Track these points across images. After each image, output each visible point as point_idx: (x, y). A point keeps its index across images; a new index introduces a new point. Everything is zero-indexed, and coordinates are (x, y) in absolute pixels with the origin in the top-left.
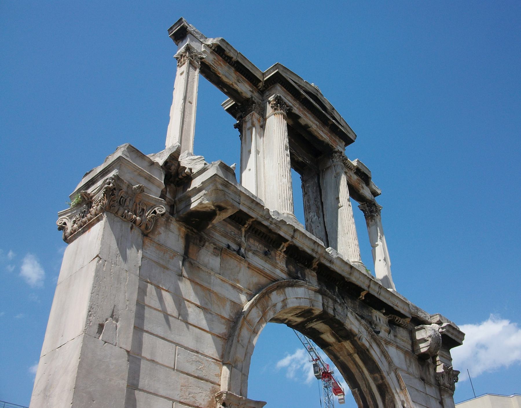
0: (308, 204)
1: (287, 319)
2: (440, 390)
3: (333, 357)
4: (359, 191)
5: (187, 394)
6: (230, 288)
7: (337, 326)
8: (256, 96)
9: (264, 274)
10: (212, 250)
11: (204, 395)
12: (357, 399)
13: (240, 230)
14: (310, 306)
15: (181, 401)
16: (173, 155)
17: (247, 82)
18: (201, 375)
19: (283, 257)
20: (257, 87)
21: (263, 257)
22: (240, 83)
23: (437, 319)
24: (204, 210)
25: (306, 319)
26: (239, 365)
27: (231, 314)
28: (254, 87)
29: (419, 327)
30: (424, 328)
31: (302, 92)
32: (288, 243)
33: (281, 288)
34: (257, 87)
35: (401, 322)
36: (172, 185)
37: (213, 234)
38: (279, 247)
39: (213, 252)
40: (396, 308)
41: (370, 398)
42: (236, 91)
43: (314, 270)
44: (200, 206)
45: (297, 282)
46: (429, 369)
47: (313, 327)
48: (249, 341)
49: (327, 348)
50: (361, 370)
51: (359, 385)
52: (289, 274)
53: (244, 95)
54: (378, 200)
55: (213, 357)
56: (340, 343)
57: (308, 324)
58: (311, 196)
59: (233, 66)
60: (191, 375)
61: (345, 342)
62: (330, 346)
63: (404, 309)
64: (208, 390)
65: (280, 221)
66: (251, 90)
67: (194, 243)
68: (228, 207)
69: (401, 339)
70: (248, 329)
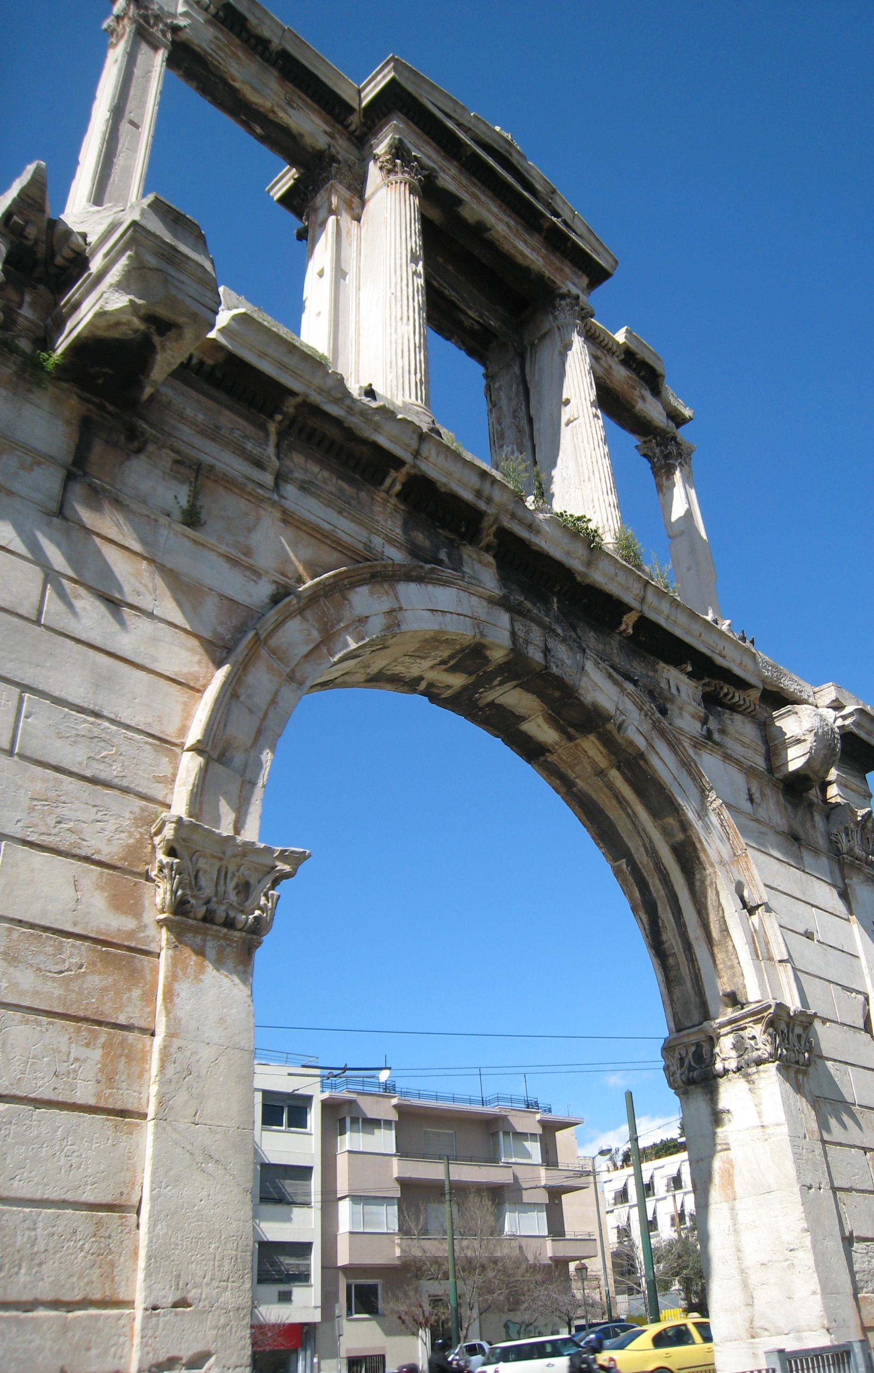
0: (499, 429)
1: (421, 678)
3: (558, 782)
4: (634, 407)
5: (51, 820)
6: (221, 563)
7: (557, 694)
8: (342, 148)
9: (333, 541)
10: (169, 465)
11: (111, 826)
12: (627, 886)
13: (263, 428)
14: (473, 634)
15: (28, 839)
16: (28, 196)
17: (315, 110)
19: (395, 510)
20: (346, 127)
21: (329, 501)
23: (830, 696)
24: (116, 334)
25: (473, 678)
26: (239, 758)
27: (220, 629)
28: (336, 125)
29: (783, 710)
30: (796, 713)
31: (462, 135)
32: (404, 470)
33: (385, 581)
34: (346, 127)
35: (736, 699)
36: (41, 287)
38: (381, 483)
39: (171, 470)
40: (719, 660)
41: (657, 882)
42: (285, 130)
43: (488, 548)
44: (102, 323)
45: (432, 570)
46: (812, 817)
47: (496, 702)
48: (272, 700)
49: (542, 759)
50: (630, 811)
51: (629, 850)
52: (414, 551)
53: (308, 140)
54: (682, 434)
55: (152, 732)
56: (572, 744)
57: (482, 692)
58: (505, 408)
60: (71, 774)
61: (584, 739)
62: (548, 754)
63: (740, 664)
64: (127, 815)
65: (377, 409)
66: (328, 129)
68: (181, 320)
69: (737, 739)
70: (270, 669)
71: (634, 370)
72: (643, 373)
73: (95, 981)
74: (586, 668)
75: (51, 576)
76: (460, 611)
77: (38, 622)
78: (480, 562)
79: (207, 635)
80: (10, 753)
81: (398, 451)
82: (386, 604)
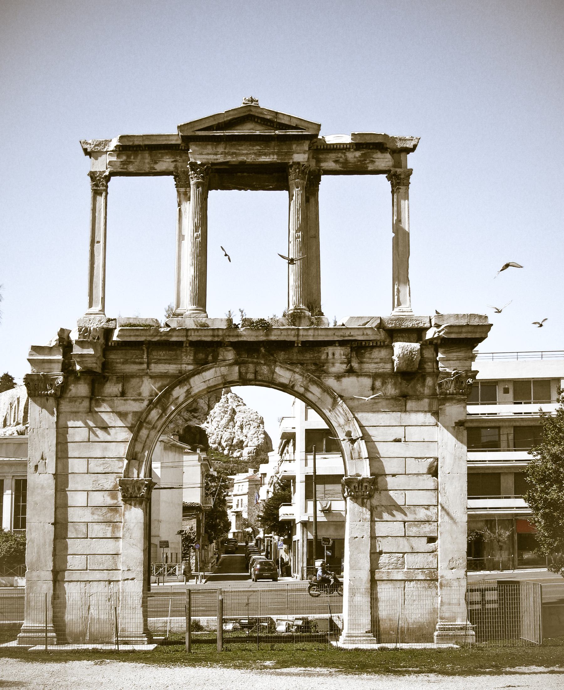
2: (439, 400)
5: (97, 485)
11: (110, 482)
18: (107, 471)
20: (182, 150)
22: (157, 163)
27: (133, 422)
37: (115, 367)
59: (145, 150)
67: (99, 383)
71: (366, 148)
72: (371, 147)
73: (109, 515)
74: (276, 370)
75: (90, 429)
76: (216, 376)
77: (89, 441)
78: (227, 351)
79: (129, 425)
80: (87, 473)
81: (180, 339)
82: (186, 388)
